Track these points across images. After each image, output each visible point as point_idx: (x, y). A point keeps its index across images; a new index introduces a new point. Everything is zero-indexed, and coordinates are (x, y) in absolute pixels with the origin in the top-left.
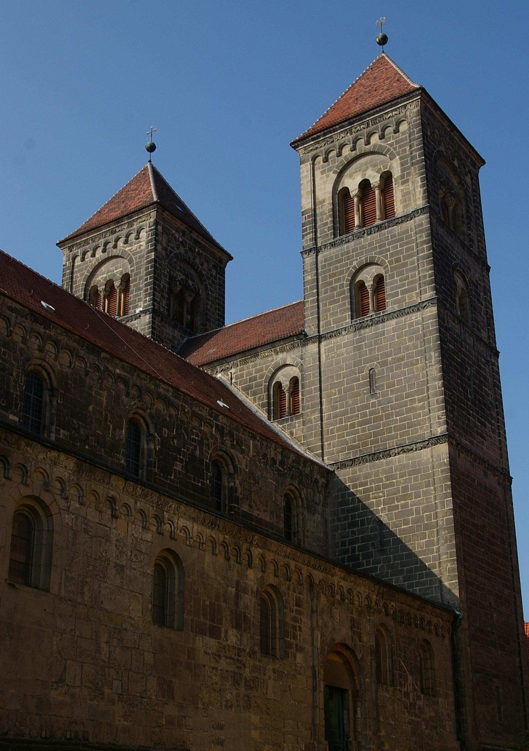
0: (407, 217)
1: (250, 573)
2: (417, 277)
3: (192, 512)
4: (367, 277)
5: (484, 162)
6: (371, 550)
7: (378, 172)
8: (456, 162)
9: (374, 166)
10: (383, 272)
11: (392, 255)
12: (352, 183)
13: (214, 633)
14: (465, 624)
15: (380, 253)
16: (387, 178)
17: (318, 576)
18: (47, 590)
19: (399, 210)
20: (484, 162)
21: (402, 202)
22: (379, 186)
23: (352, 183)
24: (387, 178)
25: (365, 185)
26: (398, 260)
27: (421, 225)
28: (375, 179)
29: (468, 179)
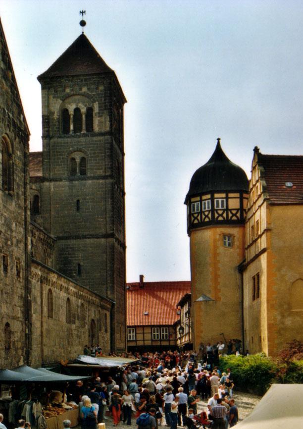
0: (100, 134)
1: (80, 301)
2: (104, 164)
3: (73, 285)
4: (78, 157)
5: (126, 102)
6: (74, 274)
7: (85, 106)
8: (118, 104)
9: (83, 103)
10: (86, 157)
11: (91, 150)
12: (71, 108)
13: (74, 323)
14: (116, 307)
15: (84, 147)
16: (90, 111)
17: (91, 297)
18: (52, 317)
19: (96, 128)
20: (126, 102)
21: (98, 125)
22: (85, 114)
23: (71, 108)
24: (90, 111)
25: (77, 110)
26: (94, 153)
27: (107, 140)
28: (83, 110)
29: (120, 110)
